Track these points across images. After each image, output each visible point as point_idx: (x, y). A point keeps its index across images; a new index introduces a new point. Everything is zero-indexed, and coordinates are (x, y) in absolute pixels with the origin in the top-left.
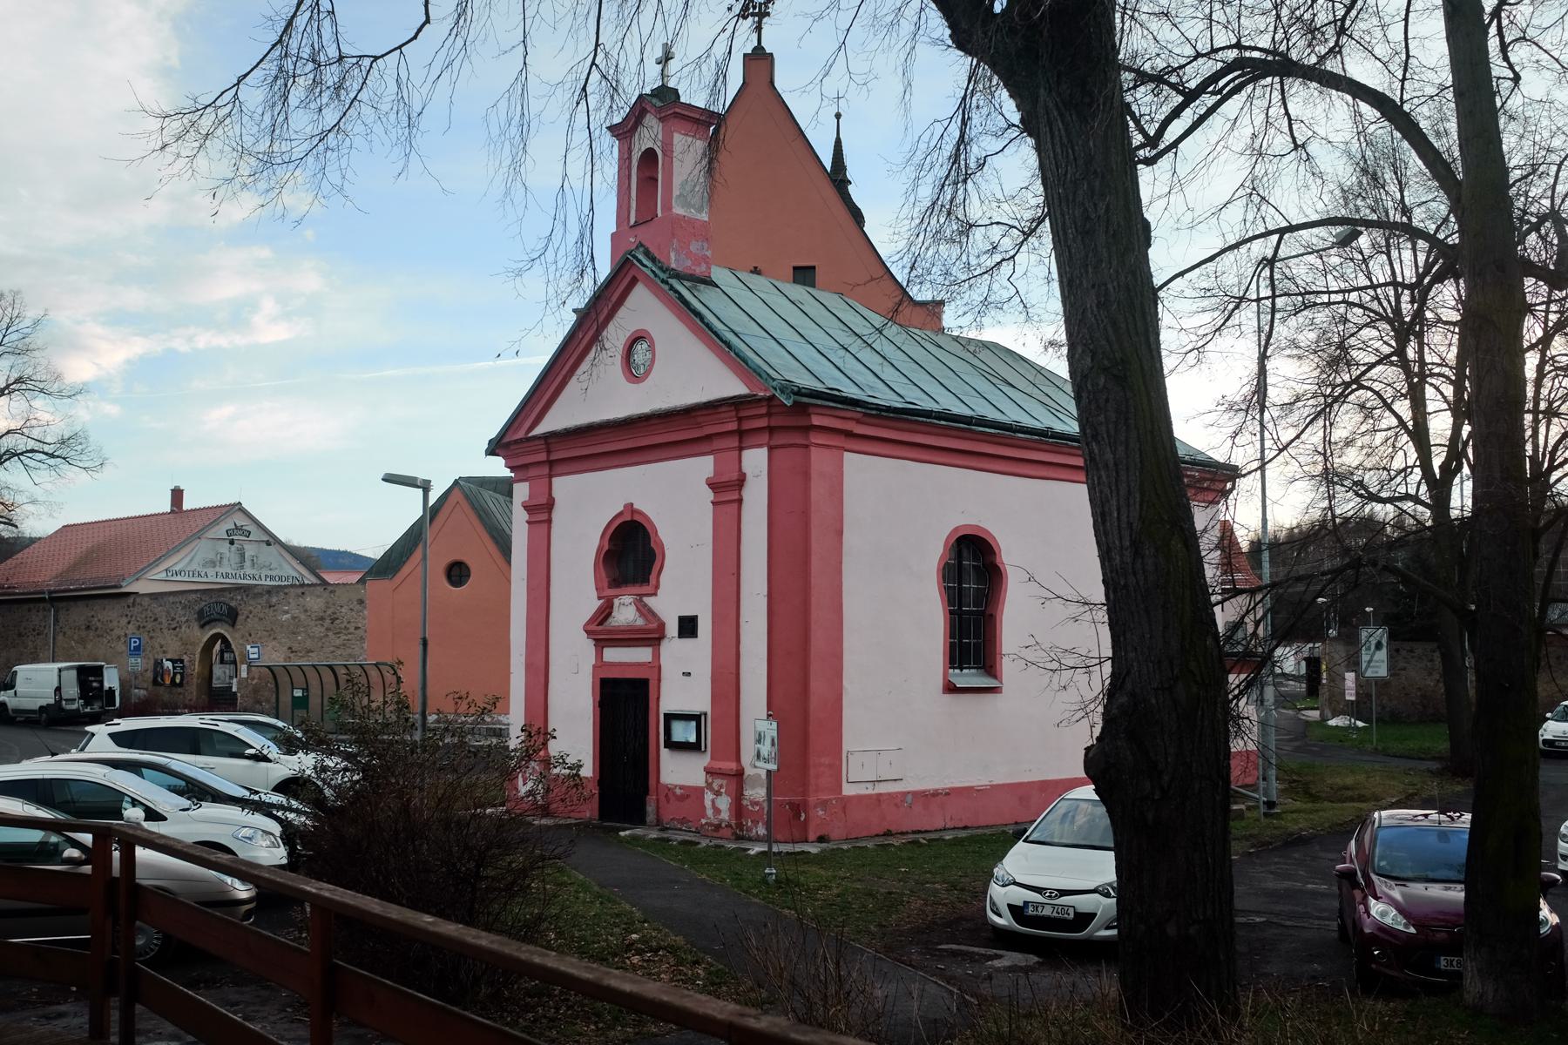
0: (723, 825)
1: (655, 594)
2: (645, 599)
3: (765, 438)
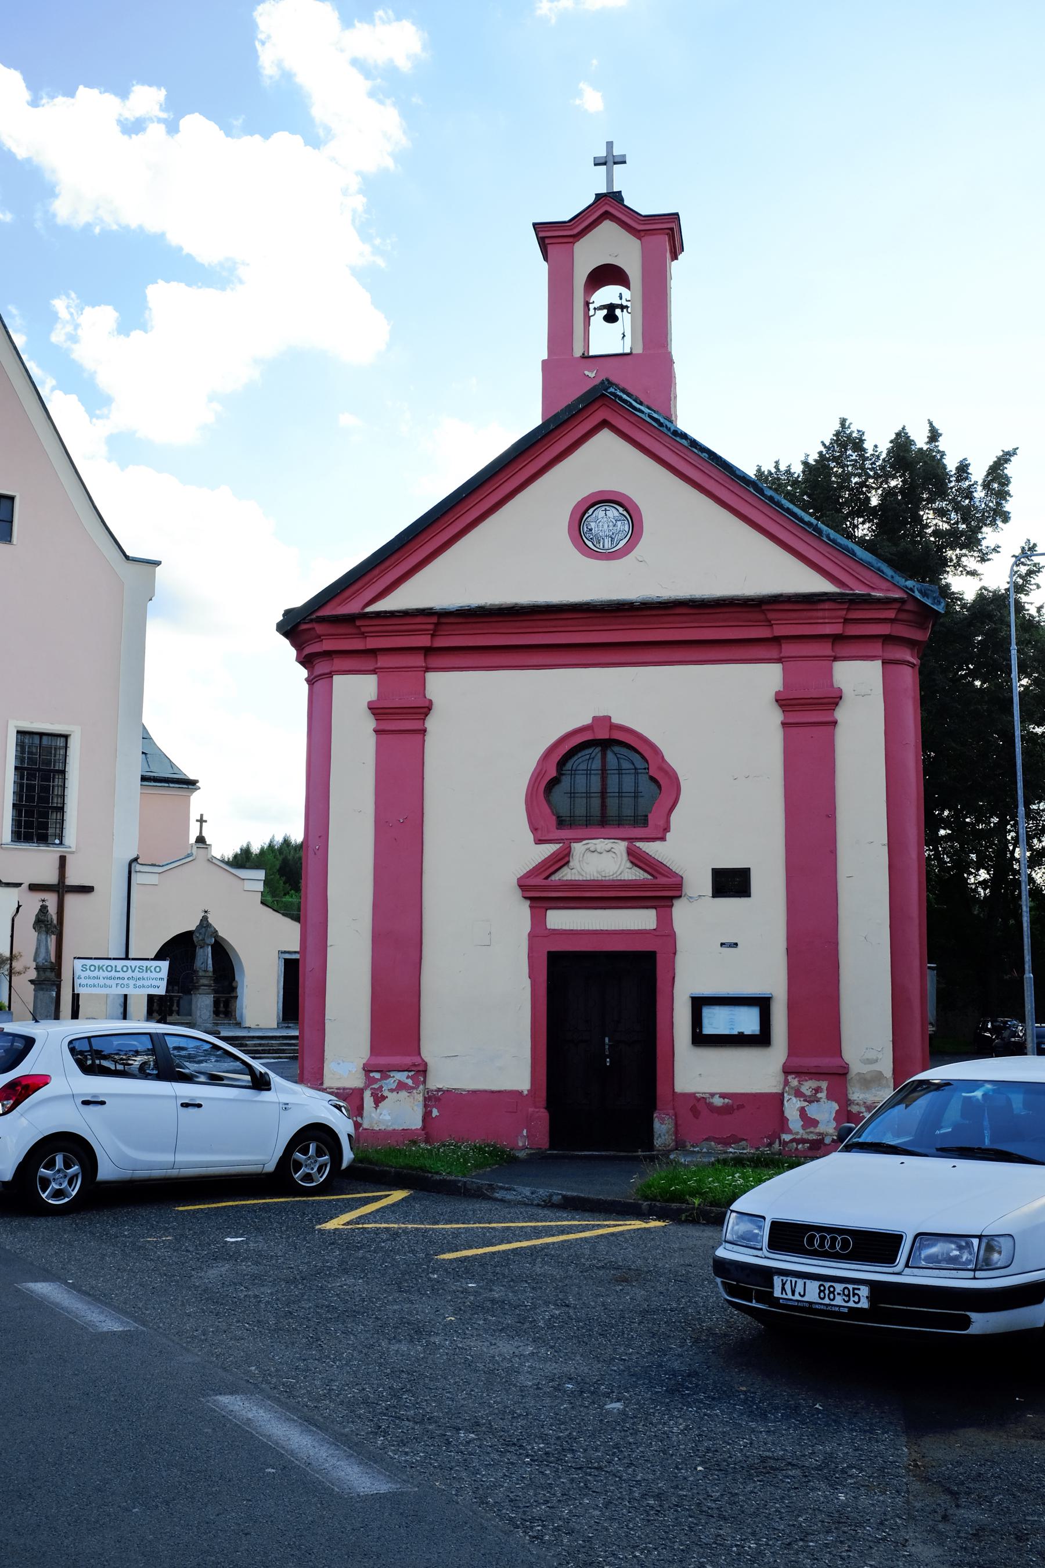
0: (828, 1141)
2: (638, 844)
3: (877, 648)
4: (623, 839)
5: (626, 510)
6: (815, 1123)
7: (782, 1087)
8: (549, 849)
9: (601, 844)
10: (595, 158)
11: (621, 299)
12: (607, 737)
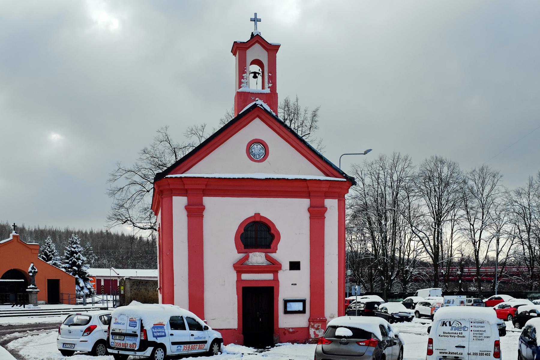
1: (275, 252)
4: (264, 252)
5: (263, 146)
6: (318, 335)
7: (308, 325)
8: (242, 255)
9: (257, 253)
10: (251, 18)
11: (259, 71)
12: (259, 220)
